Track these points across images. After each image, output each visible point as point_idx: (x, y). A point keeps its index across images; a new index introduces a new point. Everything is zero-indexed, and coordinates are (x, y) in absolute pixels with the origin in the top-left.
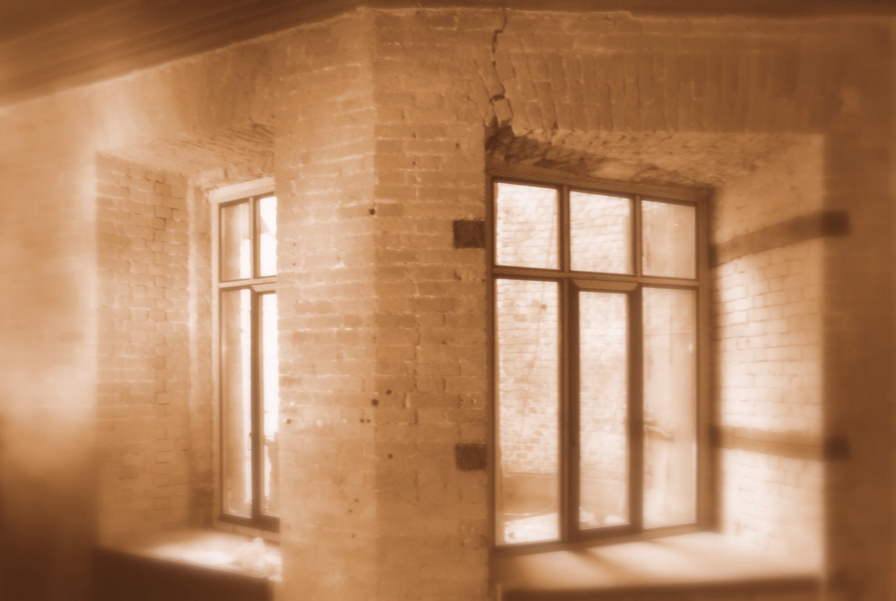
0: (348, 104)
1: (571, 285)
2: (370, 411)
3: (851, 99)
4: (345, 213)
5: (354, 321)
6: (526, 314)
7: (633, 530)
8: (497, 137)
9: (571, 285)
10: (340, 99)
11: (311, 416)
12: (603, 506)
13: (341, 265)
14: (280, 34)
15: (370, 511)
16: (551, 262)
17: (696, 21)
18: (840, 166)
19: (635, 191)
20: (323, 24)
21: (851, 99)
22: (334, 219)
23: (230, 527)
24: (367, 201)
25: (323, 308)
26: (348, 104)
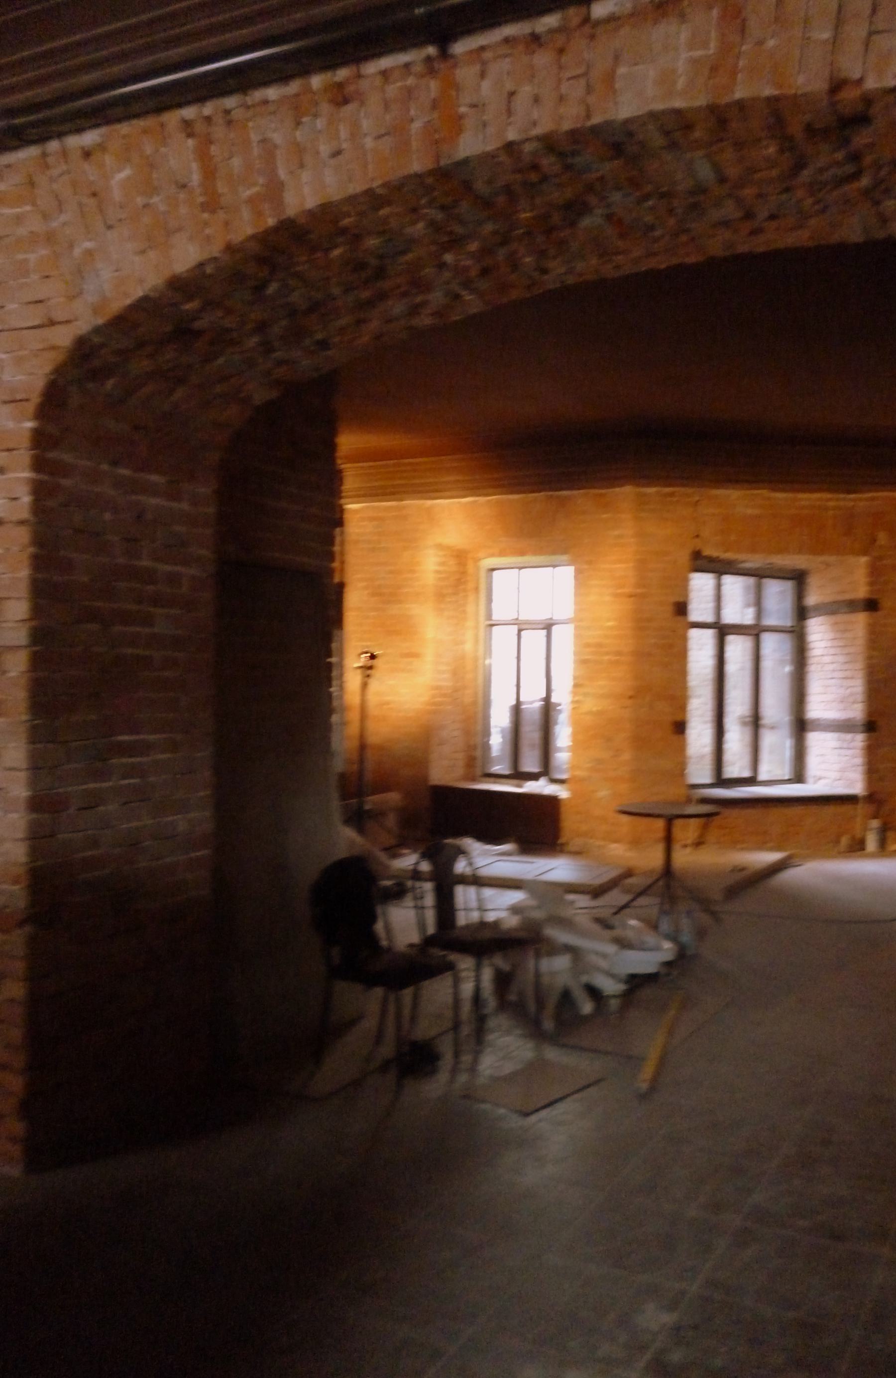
0: (620, 537)
1: (723, 631)
2: (629, 702)
3: (882, 538)
4: (616, 595)
5: (619, 653)
6: (700, 649)
7: (751, 781)
8: (697, 555)
9: (723, 631)
10: (616, 533)
11: (591, 705)
12: (736, 767)
13: (610, 624)
14: (575, 492)
15: (626, 756)
16: (709, 618)
17: (801, 496)
18: (875, 572)
19: (760, 574)
20: (603, 491)
21: (882, 538)
22: (607, 598)
23: (492, 779)
24: (627, 590)
25: (599, 645)
26: (620, 537)
